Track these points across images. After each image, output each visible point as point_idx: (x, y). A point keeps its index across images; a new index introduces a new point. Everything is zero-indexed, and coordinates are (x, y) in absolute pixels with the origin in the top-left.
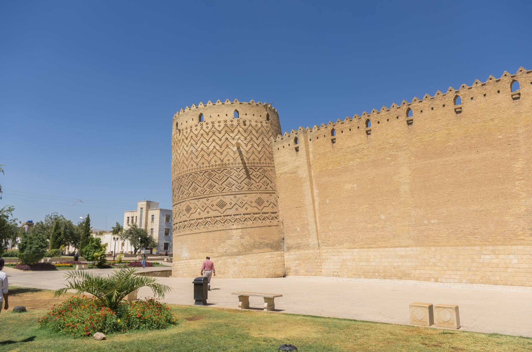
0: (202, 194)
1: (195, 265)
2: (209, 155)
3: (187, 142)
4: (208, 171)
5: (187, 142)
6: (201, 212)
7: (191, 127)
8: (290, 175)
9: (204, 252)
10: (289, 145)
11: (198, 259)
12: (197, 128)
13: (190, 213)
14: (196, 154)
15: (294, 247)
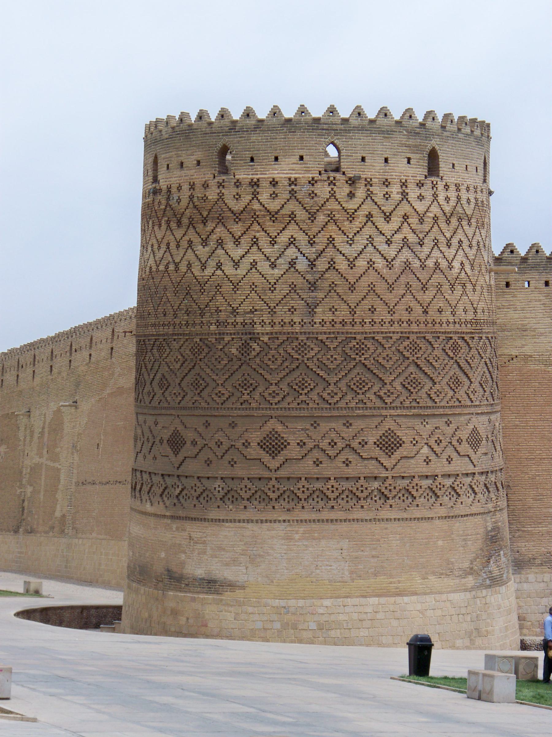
0: (436, 403)
1: (422, 613)
2: (452, 286)
3: (388, 228)
4: (451, 338)
5: (388, 228)
6: (433, 457)
7: (404, 184)
8: (543, 367)
9: (442, 574)
10: (547, 284)
11: (425, 594)
12: (423, 191)
13: (397, 454)
14: (423, 276)
15: (538, 561)
